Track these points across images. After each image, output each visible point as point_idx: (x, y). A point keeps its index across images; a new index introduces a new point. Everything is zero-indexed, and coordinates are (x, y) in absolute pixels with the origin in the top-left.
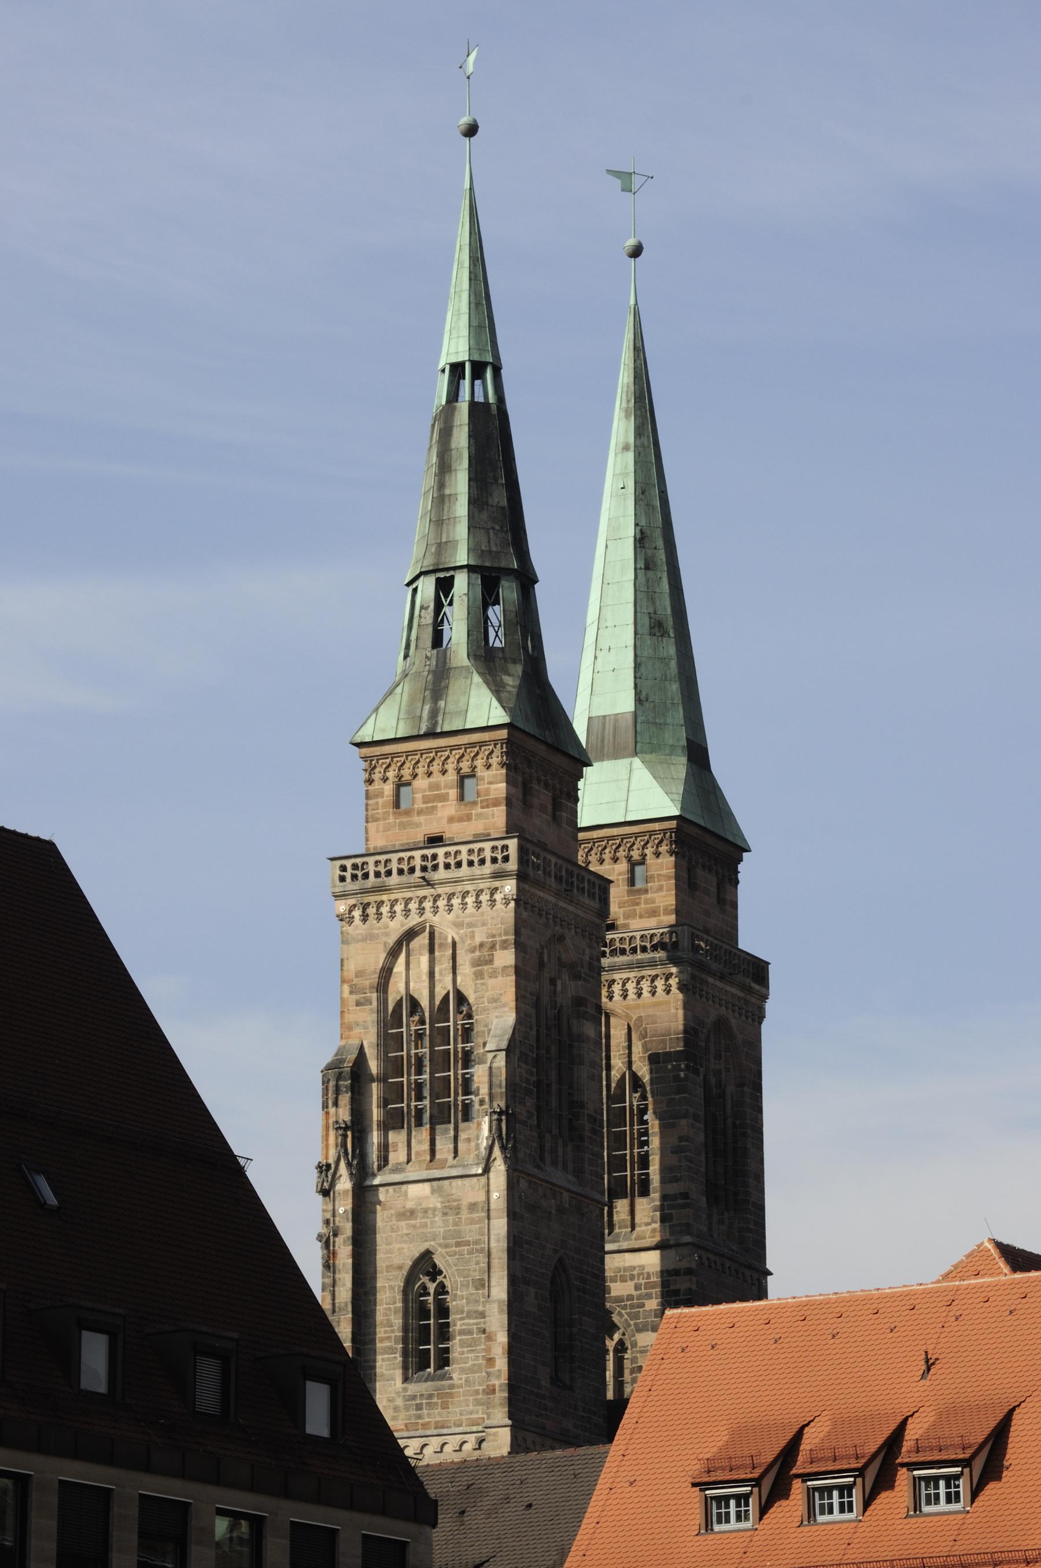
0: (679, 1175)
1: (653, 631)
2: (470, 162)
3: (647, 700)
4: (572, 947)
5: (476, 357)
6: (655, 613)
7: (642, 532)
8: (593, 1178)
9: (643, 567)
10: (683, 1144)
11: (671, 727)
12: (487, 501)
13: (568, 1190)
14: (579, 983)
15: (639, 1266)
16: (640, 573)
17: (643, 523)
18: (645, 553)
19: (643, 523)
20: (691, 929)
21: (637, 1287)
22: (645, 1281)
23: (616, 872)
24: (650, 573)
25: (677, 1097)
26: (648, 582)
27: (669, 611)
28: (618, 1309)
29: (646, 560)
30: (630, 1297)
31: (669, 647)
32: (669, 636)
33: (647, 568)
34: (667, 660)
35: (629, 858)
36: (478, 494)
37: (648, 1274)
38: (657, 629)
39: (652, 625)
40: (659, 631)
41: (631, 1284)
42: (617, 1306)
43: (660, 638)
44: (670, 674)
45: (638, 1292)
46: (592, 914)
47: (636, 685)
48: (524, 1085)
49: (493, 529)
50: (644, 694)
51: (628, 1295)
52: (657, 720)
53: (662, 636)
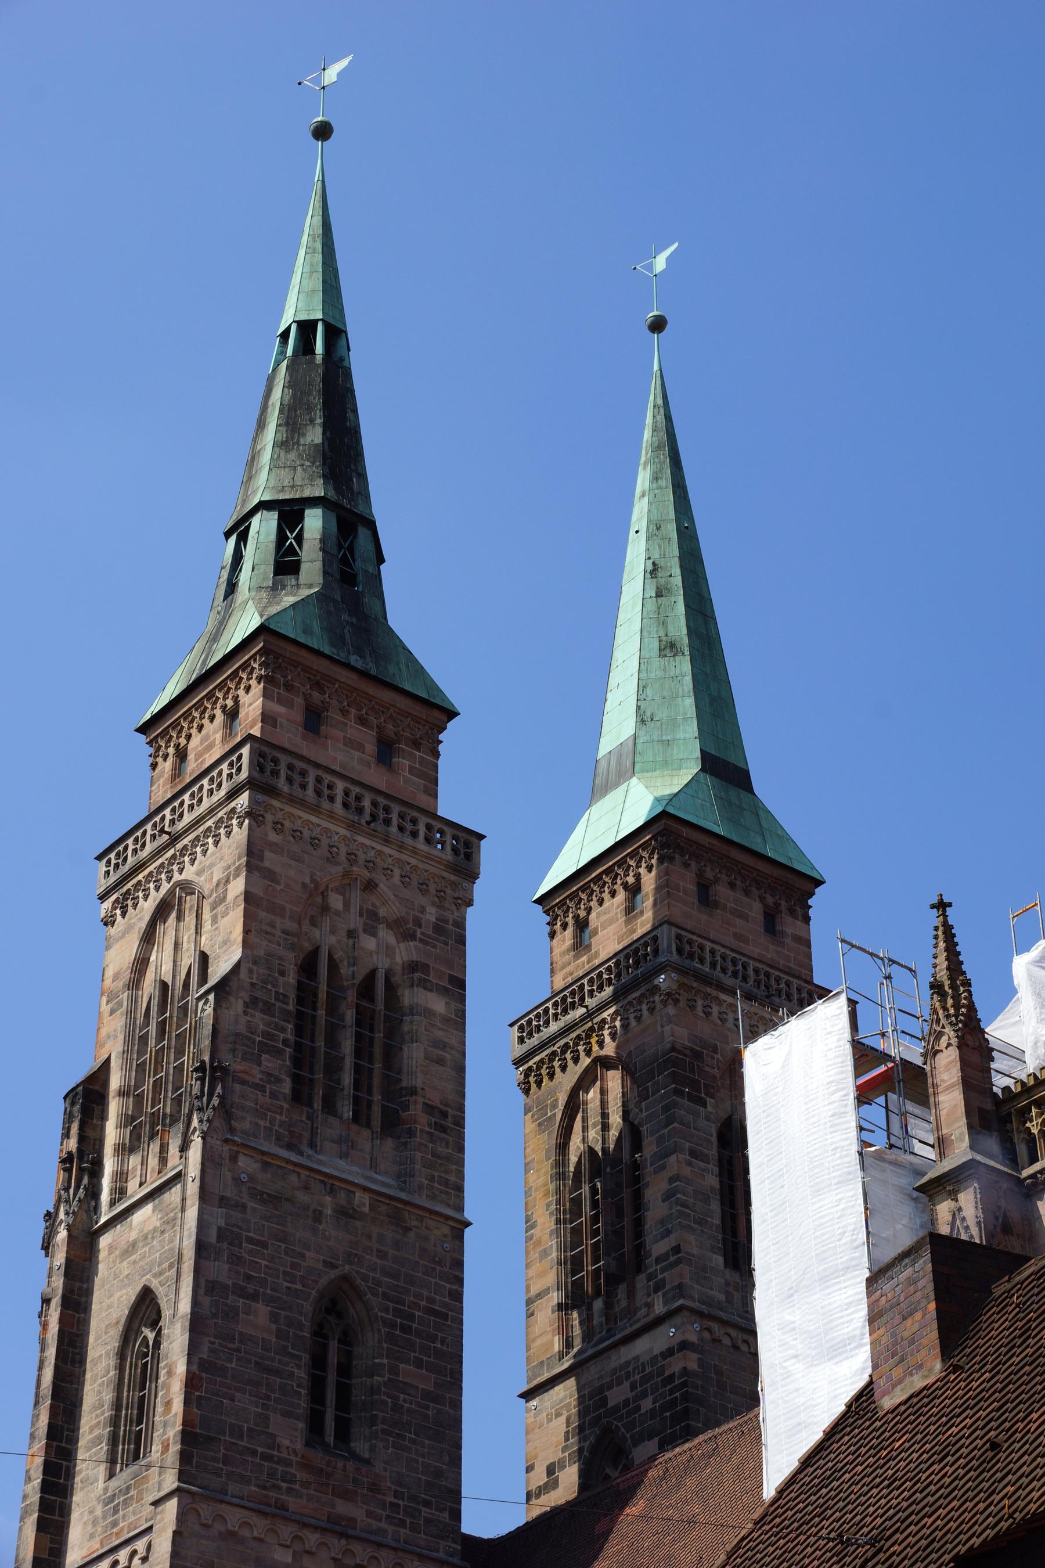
0: (670, 1226)
1: (662, 653)
2: (322, 159)
3: (652, 720)
4: (393, 897)
5: (303, 317)
6: (667, 635)
7: (654, 564)
8: (436, 1185)
9: (654, 595)
10: (674, 1185)
11: (681, 741)
12: (298, 440)
13: (366, 1189)
14: (411, 944)
15: (634, 1358)
16: (648, 602)
18: (657, 583)
19: (656, 555)
20: (674, 930)
21: (633, 1387)
22: (641, 1375)
23: (615, 905)
24: (660, 600)
25: (666, 1131)
26: (659, 608)
27: (684, 631)
28: (615, 1423)
29: (658, 588)
30: (626, 1402)
31: (683, 665)
32: (683, 654)
33: (659, 595)
34: (679, 678)
35: (625, 886)
36: (287, 437)
37: (643, 1364)
38: (668, 650)
39: (663, 647)
40: (671, 651)
41: (627, 1384)
42: (615, 1419)
43: (672, 658)
44: (683, 690)
45: (634, 1393)
46: (442, 867)
47: (638, 707)
48: (258, 1039)
49: (302, 465)
50: (648, 714)
51: (624, 1401)
52: (664, 738)
53: (674, 656)
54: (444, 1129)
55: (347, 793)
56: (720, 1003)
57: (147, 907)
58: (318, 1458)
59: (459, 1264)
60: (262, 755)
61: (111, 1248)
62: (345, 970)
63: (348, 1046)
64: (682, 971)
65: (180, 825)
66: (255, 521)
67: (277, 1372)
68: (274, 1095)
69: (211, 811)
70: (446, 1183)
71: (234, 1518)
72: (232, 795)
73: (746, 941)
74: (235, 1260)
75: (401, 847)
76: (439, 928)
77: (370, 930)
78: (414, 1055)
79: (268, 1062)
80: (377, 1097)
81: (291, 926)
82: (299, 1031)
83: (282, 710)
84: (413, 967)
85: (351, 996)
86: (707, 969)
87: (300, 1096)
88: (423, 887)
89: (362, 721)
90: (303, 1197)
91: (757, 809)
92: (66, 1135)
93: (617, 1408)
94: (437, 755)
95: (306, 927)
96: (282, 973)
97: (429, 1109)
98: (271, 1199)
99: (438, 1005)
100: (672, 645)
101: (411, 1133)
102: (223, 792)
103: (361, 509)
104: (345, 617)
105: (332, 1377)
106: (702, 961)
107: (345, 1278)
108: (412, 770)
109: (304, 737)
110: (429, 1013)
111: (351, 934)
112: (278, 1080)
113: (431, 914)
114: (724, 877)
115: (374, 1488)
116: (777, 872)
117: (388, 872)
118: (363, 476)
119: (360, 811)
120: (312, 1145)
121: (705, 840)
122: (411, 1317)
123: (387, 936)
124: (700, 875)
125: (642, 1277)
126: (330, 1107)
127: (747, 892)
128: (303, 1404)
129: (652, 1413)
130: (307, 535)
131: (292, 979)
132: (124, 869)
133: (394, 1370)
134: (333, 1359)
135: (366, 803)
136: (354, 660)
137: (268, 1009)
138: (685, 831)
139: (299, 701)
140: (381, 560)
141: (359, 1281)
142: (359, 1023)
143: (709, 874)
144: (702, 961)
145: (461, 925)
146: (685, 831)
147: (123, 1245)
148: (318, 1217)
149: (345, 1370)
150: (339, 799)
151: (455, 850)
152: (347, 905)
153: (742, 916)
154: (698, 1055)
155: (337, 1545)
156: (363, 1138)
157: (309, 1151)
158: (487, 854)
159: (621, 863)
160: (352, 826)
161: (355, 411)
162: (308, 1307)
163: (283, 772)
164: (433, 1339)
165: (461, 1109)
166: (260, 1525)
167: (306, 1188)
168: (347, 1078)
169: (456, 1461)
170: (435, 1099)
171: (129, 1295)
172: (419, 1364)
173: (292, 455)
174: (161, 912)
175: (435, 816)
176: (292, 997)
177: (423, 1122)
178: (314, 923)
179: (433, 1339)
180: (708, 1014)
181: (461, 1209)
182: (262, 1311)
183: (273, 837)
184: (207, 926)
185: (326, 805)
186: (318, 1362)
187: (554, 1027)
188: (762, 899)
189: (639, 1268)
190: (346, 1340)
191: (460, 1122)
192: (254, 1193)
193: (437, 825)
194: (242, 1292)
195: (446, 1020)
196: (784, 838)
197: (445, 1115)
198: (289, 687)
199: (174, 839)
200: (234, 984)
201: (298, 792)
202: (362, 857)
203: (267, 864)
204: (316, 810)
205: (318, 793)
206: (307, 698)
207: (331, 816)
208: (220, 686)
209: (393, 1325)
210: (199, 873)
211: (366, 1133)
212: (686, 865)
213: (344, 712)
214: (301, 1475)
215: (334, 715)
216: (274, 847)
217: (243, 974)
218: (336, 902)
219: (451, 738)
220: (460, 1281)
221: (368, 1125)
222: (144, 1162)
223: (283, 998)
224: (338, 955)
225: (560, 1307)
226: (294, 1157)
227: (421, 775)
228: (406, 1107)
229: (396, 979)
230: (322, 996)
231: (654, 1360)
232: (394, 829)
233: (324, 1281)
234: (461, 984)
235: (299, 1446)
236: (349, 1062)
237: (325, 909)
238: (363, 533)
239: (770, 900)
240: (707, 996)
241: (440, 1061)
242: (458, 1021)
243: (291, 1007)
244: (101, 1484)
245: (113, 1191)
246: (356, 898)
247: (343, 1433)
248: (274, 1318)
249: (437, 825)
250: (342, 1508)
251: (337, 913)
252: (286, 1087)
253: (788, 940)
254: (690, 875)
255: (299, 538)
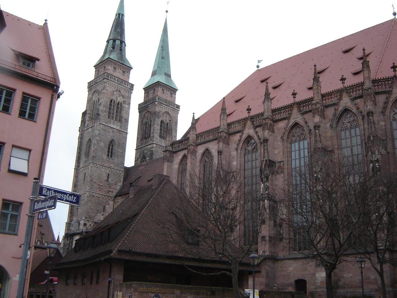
14: (125, 99)
17: (163, 45)
33: (162, 50)
54: (126, 122)
55: (118, 79)
56: (163, 106)
57: (93, 91)
58: (108, 159)
59: (126, 138)
60: (107, 75)
61: (86, 132)
62: (115, 102)
63: (115, 111)
64: (158, 102)
65: (97, 82)
66: (110, 41)
67: (104, 150)
68: (106, 117)
69: (101, 81)
70: (126, 128)
71: (98, 166)
72: (103, 79)
73: (167, 97)
74: (100, 137)
75: (124, 86)
76: (128, 97)
77: (119, 97)
78: (123, 112)
79: (105, 113)
80: (118, 118)
81: (109, 96)
82: (109, 109)
83: (110, 68)
84: (124, 101)
85: (116, 105)
86: (161, 102)
87: (109, 117)
88: (126, 92)
89: (121, 69)
90: (108, 130)
91: (171, 80)
92: (82, 118)
93: (145, 153)
94: (130, 73)
95: (111, 96)
96: (108, 102)
97: (125, 119)
98: (104, 130)
99: (127, 106)
100: (163, 57)
101: (122, 122)
102: (102, 79)
103: (123, 40)
104: (120, 55)
105: (110, 150)
106: (161, 100)
107: (113, 139)
108: (126, 76)
109: (113, 72)
110: (125, 107)
111: (117, 97)
112: (106, 116)
113: (127, 95)
114: (166, 89)
115: (114, 163)
116: (173, 89)
117: (122, 90)
118: (124, 35)
119: (119, 82)
120: (110, 123)
121: (164, 85)
122: (120, 144)
123: (122, 98)
124: (163, 89)
125: (150, 138)
126: (112, 118)
127: (168, 91)
128: (107, 153)
129: (149, 154)
130: (116, 44)
131: (109, 103)
132: (91, 85)
133: (118, 150)
134: (111, 148)
135: (120, 81)
136: (120, 62)
137: (106, 107)
138: (161, 84)
139: (113, 67)
140: (125, 46)
141: (114, 140)
142: (117, 108)
143: (164, 89)
144: (161, 100)
145: (131, 96)
146: (161, 84)
147: (88, 132)
148: (110, 132)
149: (112, 149)
150: (117, 80)
151: (131, 87)
152: (117, 93)
153: (168, 94)
154: (159, 112)
155: (110, 169)
156: (116, 122)
157: (109, 124)
158: (135, 87)
159: (153, 86)
160: (118, 84)
161: (124, 26)
162: (108, 142)
163: (110, 77)
164: (123, 146)
165: (128, 119)
166: (101, 167)
167: (109, 129)
168: (115, 115)
169: (124, 160)
170: (125, 118)
171: (88, 138)
172: (121, 149)
173: (116, 32)
174: (95, 91)
175: (129, 83)
176: (109, 105)
177: (124, 121)
178: (112, 96)
179: (123, 146)
180: (161, 107)
181: (127, 131)
182: (103, 143)
183: (108, 85)
184: (99, 95)
185: (115, 81)
186: (109, 148)
187: (143, 106)
188: (170, 92)
189: (150, 137)
190: (112, 146)
191: (128, 121)
192: (102, 129)
193: (129, 83)
194: (100, 141)
195: (128, 108)
196: (174, 84)
197: (126, 120)
198: (112, 65)
199: (97, 83)
200: (102, 104)
201: (111, 79)
202: (119, 87)
203: (107, 89)
204: (113, 82)
205: (114, 79)
206: (114, 66)
207: (115, 83)
208: (104, 63)
209: (118, 145)
210: (99, 88)
211: (117, 122)
212: (161, 88)
213: (118, 68)
214: (106, 161)
215: (117, 68)
216: (108, 86)
217: (103, 102)
218: (115, 93)
219: (132, 71)
220: (126, 140)
221: (117, 121)
222: (90, 123)
223: (107, 105)
224: (115, 100)
225: (140, 140)
226: (107, 125)
227: (128, 76)
228: (122, 119)
229: (122, 103)
230: (113, 105)
231: (150, 148)
232: (123, 84)
233: (110, 140)
234: (130, 104)
235: (106, 158)
236: (115, 113)
237: (114, 94)
238: (123, 43)
239: (171, 92)
240: (161, 105)
241: (126, 113)
242: (129, 108)
243: (109, 106)
244: (84, 159)
245: (87, 125)
246: (118, 92)
247: (111, 156)
248: (104, 144)
249: (129, 83)
250: (110, 165)
251: (115, 95)
252: (107, 116)
253: (173, 97)
254: (161, 89)
255: (115, 44)
